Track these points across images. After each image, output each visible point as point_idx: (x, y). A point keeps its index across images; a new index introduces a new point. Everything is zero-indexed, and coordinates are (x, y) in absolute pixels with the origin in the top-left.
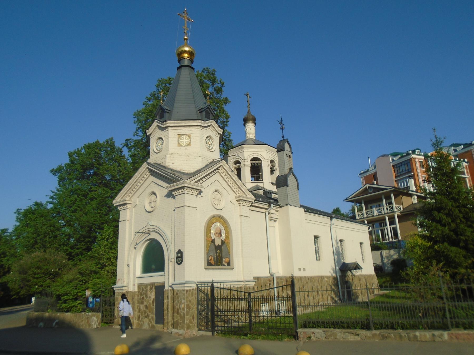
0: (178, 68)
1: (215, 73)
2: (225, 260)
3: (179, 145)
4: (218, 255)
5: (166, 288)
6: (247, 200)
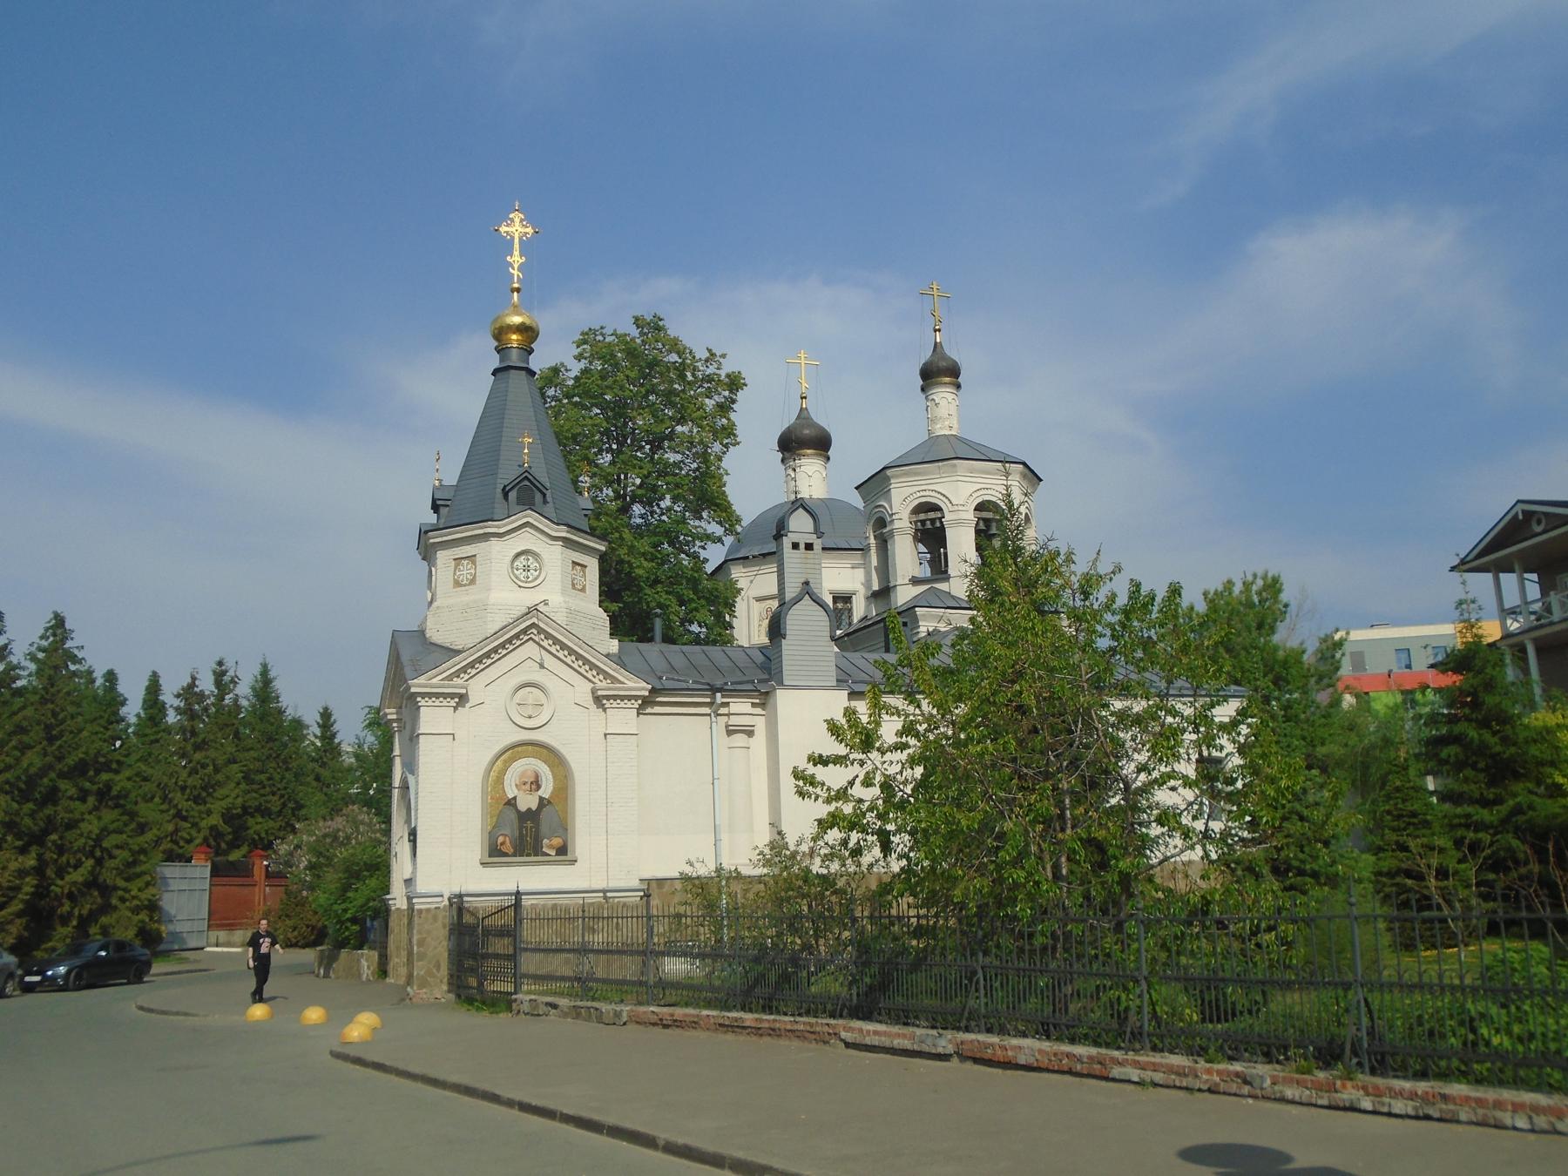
0: (494, 373)
3: (457, 584)
4: (528, 831)
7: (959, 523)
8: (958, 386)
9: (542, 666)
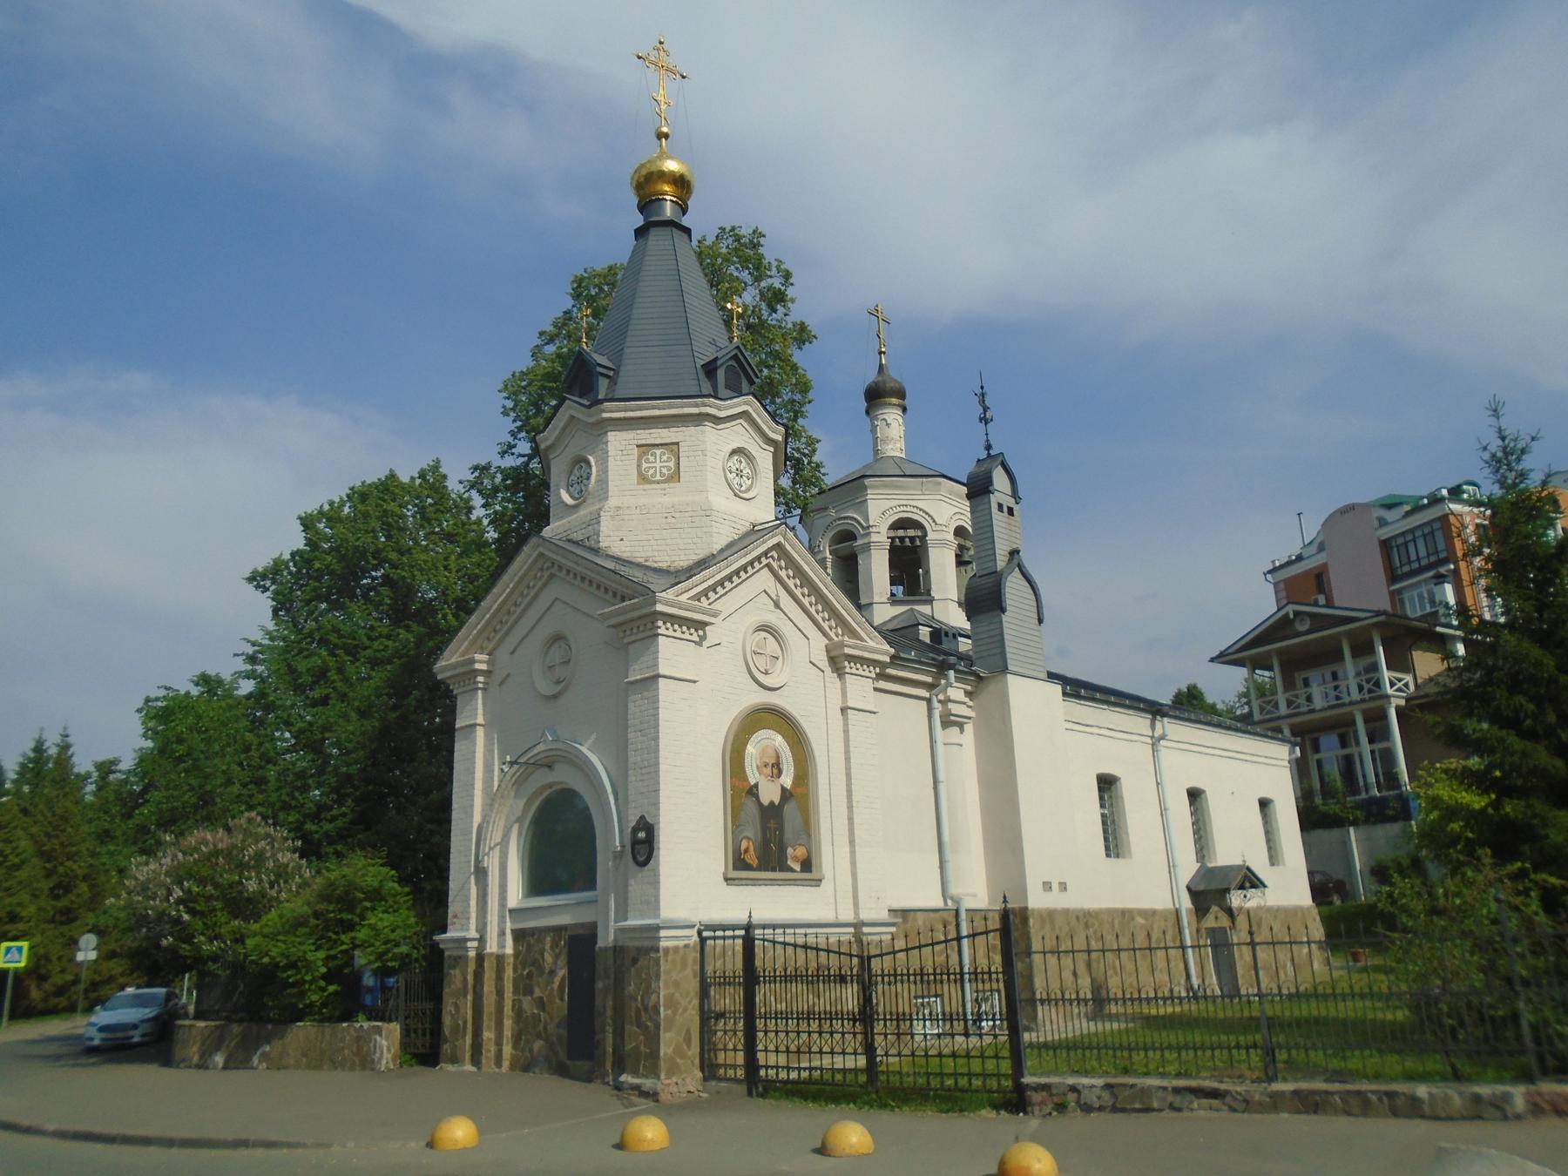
0: (640, 233)
1: (762, 240)
2: (794, 853)
3: (643, 479)
4: (771, 837)
5: (601, 943)
6: (866, 655)
7: (943, 543)
9: (777, 605)
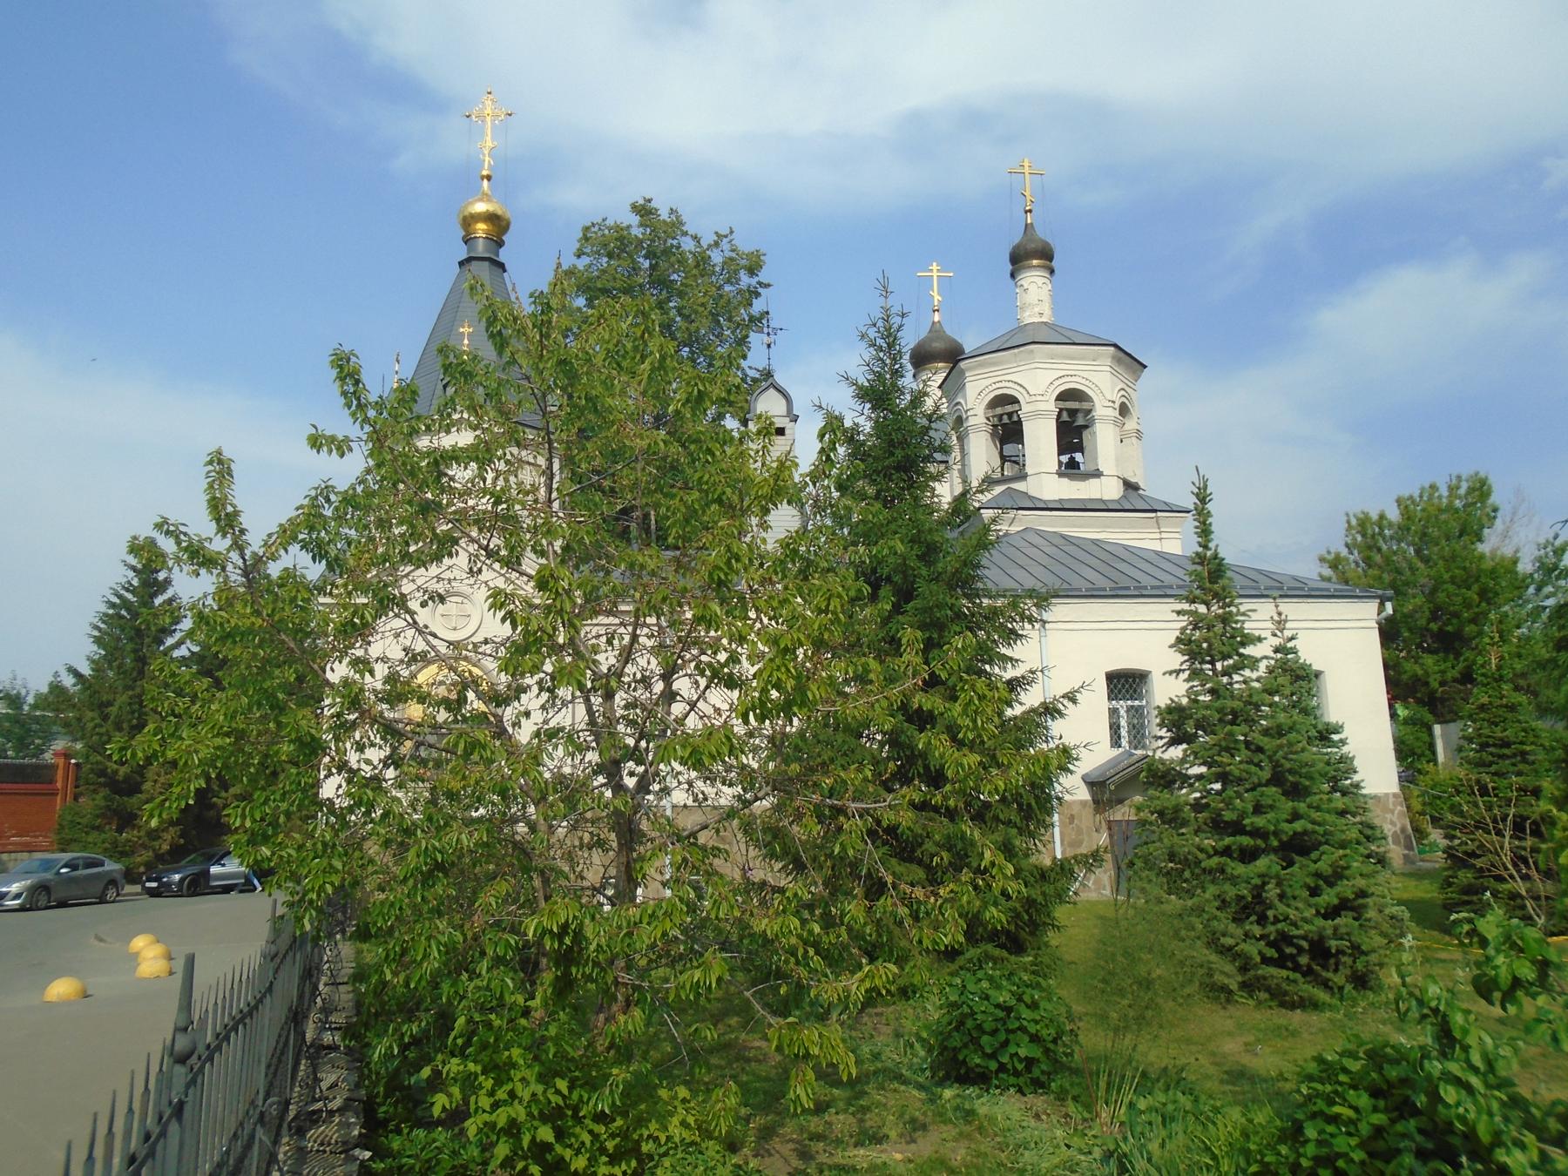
7: (1037, 414)
8: (1052, 272)
